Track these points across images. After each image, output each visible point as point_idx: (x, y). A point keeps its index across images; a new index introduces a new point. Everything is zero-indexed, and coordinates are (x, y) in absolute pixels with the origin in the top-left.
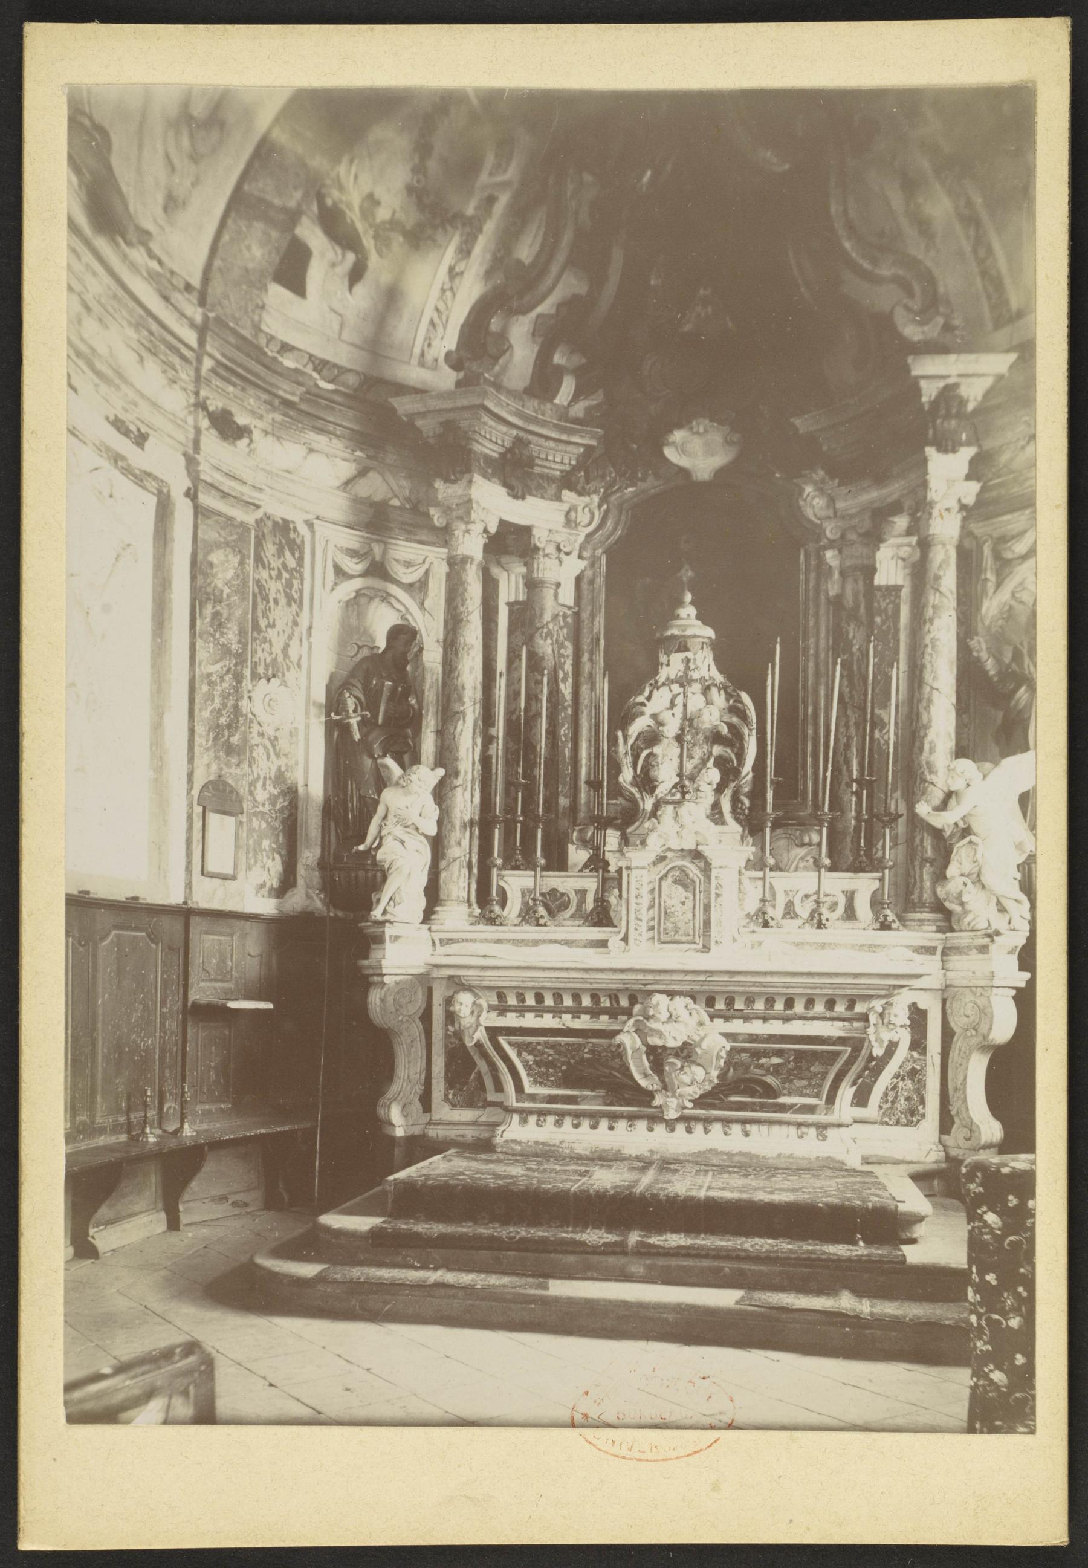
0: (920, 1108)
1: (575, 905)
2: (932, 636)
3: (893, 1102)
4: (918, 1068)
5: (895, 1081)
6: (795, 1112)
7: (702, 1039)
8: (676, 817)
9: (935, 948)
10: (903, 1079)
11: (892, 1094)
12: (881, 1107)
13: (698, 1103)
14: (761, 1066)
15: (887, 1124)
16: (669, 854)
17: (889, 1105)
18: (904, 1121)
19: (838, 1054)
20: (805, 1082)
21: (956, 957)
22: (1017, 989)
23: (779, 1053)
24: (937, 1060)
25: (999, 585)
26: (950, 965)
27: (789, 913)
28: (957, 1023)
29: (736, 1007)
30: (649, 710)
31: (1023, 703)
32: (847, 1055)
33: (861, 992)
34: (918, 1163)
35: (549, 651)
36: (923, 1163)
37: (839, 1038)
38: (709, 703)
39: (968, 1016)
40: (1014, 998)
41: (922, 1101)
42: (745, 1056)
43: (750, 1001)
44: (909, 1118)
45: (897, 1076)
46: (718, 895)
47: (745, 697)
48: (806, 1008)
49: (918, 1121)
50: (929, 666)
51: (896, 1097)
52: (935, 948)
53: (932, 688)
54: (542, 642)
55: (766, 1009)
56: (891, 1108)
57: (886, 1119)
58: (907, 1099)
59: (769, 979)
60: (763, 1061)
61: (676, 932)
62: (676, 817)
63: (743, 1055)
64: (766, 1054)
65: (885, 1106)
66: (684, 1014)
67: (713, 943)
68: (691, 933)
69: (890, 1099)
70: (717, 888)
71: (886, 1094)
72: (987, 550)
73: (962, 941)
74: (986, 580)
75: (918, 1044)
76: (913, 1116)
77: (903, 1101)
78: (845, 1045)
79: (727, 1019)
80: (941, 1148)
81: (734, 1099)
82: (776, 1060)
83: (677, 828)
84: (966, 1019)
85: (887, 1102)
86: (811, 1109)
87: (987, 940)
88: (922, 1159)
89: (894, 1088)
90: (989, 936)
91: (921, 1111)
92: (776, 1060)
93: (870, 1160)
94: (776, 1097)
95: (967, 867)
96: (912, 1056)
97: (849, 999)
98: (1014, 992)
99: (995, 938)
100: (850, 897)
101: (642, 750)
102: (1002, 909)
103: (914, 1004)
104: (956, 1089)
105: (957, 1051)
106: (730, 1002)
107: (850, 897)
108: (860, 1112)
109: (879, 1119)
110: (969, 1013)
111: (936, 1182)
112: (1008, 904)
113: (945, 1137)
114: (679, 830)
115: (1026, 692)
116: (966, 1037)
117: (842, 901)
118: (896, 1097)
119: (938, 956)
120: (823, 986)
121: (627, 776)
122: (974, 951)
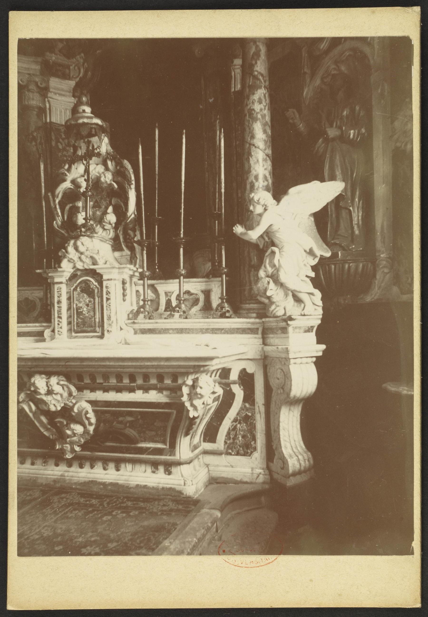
0: (253, 443)
1: (39, 307)
2: (249, 107)
3: (234, 439)
4: (250, 414)
5: (235, 424)
6: (149, 454)
7: (74, 404)
8: (76, 248)
9: (258, 329)
10: (240, 423)
11: (232, 433)
12: (225, 442)
13: (84, 447)
14: (121, 422)
15: (230, 454)
16: (79, 273)
17: (231, 441)
18: (242, 452)
19: (168, 415)
20: (153, 433)
21: (271, 336)
22: (316, 357)
23: (130, 414)
24: (262, 409)
25: (313, 75)
26: (269, 341)
27: (169, 308)
28: (274, 383)
29: (98, 381)
30: (70, 177)
31: (321, 150)
32: (174, 415)
33: (183, 370)
34: (251, 483)
35: (34, 149)
36: (255, 483)
37: (166, 403)
38: (107, 169)
39: (278, 379)
40: (315, 363)
41: (254, 438)
42: (108, 416)
43: (106, 377)
44: (245, 450)
45: (235, 420)
46: (108, 299)
47: (127, 164)
48: (145, 381)
49: (252, 452)
50: (247, 129)
51: (236, 435)
52: (258, 329)
53: (250, 144)
54: (29, 144)
55: (118, 382)
56: (233, 443)
57: (230, 451)
58: (243, 437)
59: (108, 363)
60: (121, 419)
61: (84, 325)
62: (76, 248)
63: (107, 415)
64: (121, 414)
65: (228, 442)
66: (57, 389)
67: (106, 332)
68: (93, 325)
69: (232, 436)
70: (107, 294)
71: (228, 434)
72: (304, 54)
73: (272, 324)
74: (305, 73)
75: (249, 397)
76: (247, 449)
77: (240, 438)
78: (171, 409)
79: (93, 390)
80: (267, 472)
81: (108, 444)
82: (129, 419)
83: (78, 254)
84: (277, 381)
85: (229, 438)
86: (159, 452)
87: (283, 324)
88: (254, 481)
89: (235, 428)
90: (285, 321)
91: (254, 446)
92: (129, 419)
93: (218, 481)
94: (135, 444)
95: (270, 270)
96: (245, 406)
97: (171, 374)
98: (314, 359)
99: (289, 322)
100: (207, 293)
101: (66, 205)
102: (298, 300)
103: (244, 369)
104: (275, 431)
105: (274, 403)
106: (93, 378)
107: (207, 293)
108: (208, 446)
109: (225, 451)
110: (279, 376)
111: (263, 499)
112: (304, 297)
113: (271, 464)
114: (80, 255)
115: (323, 142)
116: (278, 394)
117: (202, 297)
118: (236, 435)
119: (260, 336)
120: (141, 367)
121: (58, 221)
122: (280, 331)
